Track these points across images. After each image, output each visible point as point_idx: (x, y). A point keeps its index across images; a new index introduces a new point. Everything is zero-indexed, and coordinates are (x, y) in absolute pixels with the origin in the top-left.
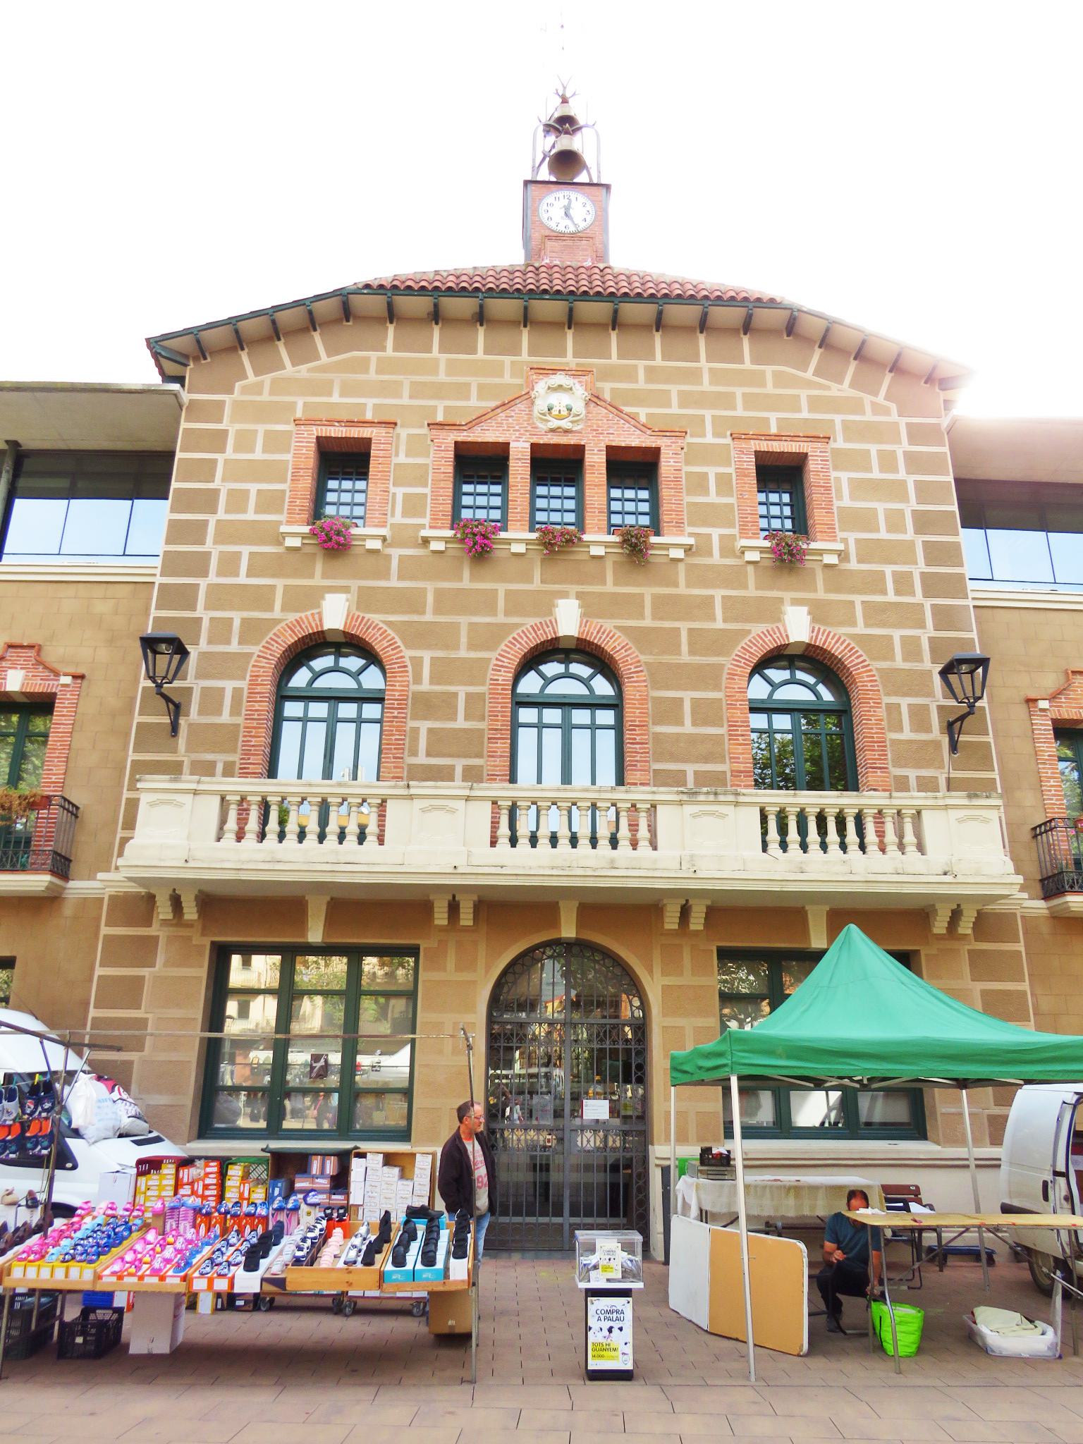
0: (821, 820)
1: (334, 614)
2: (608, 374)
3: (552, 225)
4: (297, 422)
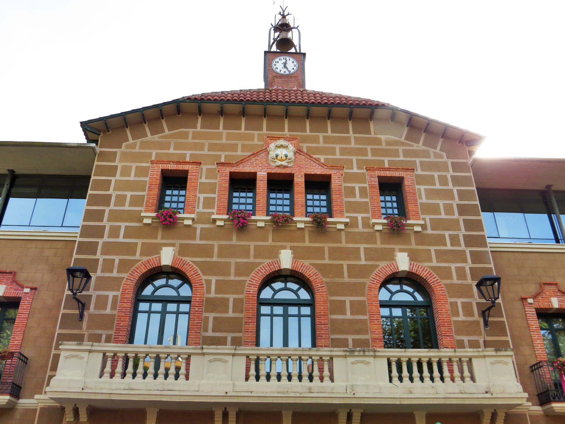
0: (420, 364)
1: (167, 257)
2: (305, 140)
3: (278, 71)
4: (152, 162)
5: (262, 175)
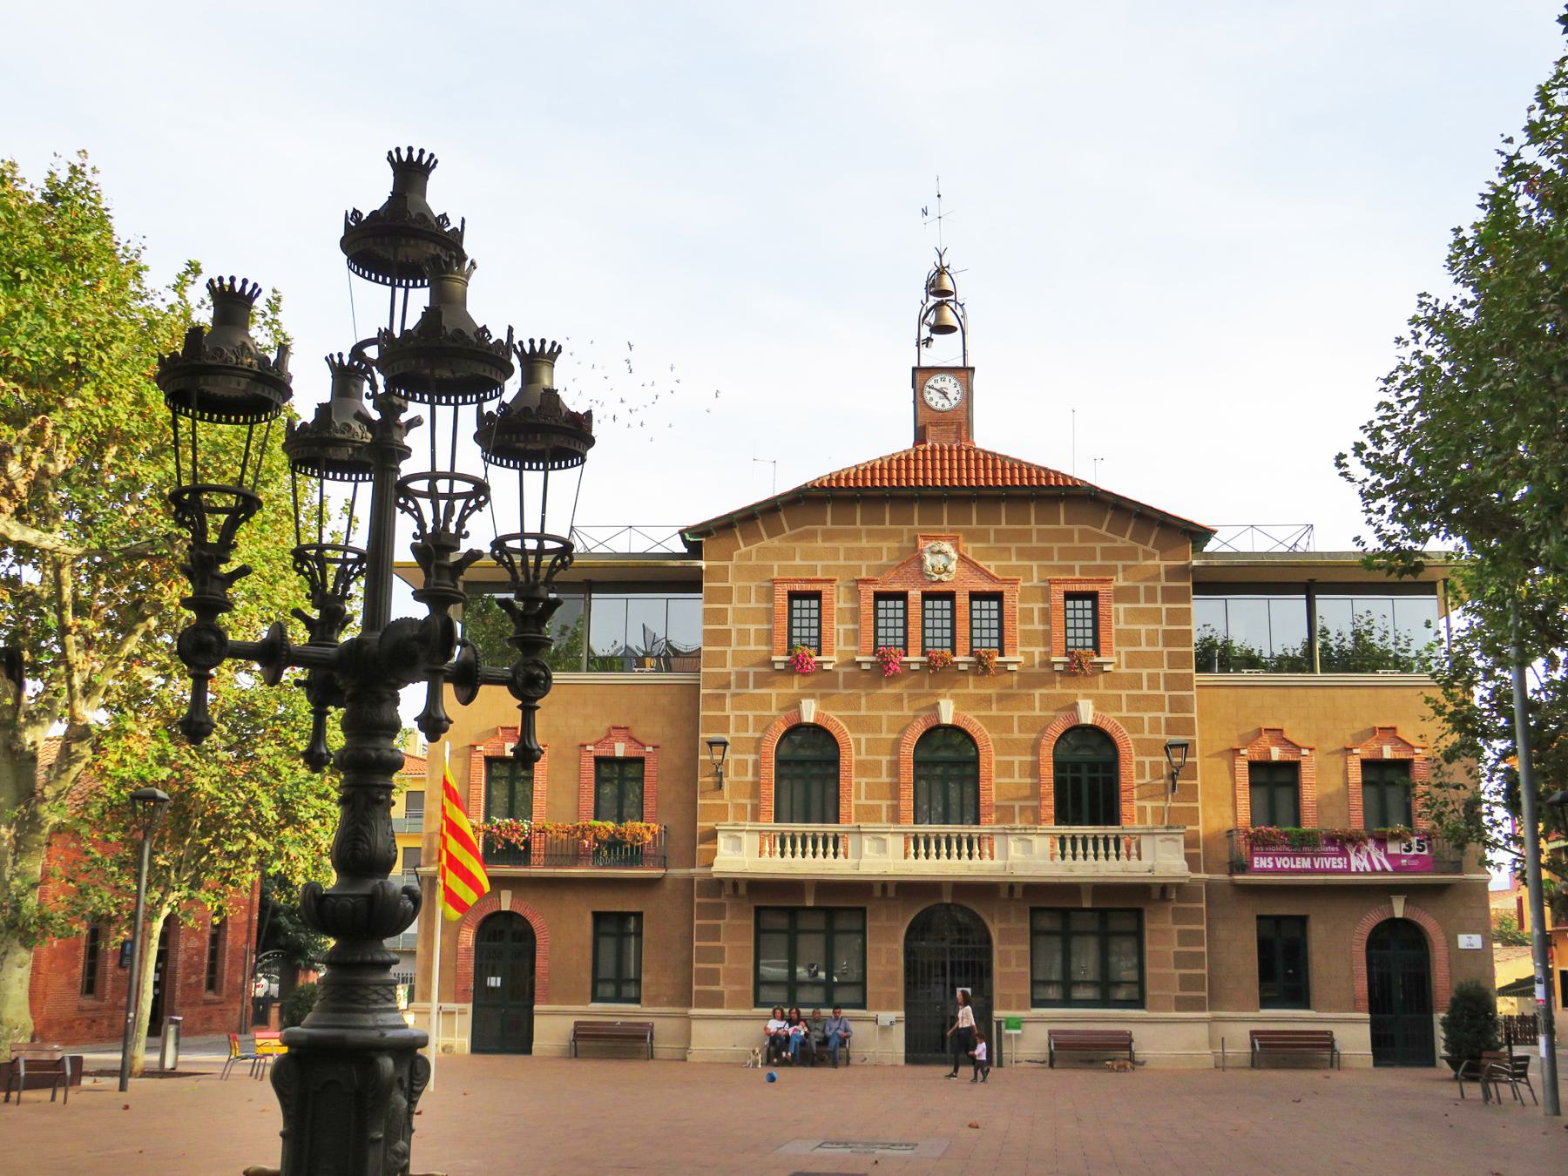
5: (915, 594)
